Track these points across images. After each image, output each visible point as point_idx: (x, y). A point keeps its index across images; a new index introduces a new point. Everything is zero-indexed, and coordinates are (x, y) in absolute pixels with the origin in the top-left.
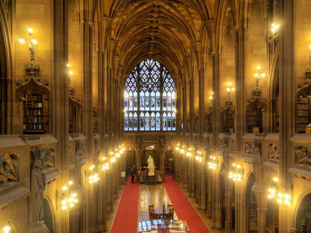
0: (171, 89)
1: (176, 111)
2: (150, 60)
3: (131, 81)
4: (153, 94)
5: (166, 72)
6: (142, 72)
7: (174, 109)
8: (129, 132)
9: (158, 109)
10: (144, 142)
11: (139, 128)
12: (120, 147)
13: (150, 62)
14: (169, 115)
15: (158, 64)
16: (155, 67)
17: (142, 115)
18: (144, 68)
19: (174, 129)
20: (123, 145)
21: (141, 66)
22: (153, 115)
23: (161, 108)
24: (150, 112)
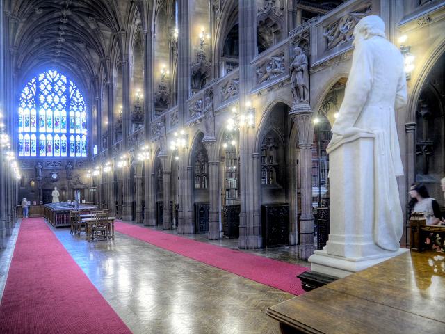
0: (81, 108)
1: (86, 134)
2: (53, 72)
3: (27, 93)
4: (57, 113)
5: (74, 87)
7: (85, 131)
9: (64, 131)
11: (38, 153)
14: (78, 138)
15: (64, 78)
22: (57, 138)
24: (53, 134)
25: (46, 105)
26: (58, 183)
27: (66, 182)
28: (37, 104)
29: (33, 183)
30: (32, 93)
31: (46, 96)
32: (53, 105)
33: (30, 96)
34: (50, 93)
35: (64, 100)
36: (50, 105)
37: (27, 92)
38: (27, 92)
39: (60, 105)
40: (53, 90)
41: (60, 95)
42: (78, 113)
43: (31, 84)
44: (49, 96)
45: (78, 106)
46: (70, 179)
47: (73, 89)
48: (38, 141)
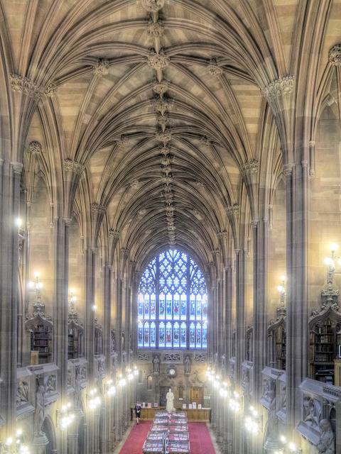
3: (147, 276)
4: (176, 297)
6: (162, 268)
7: (205, 318)
8: (144, 348)
9: (184, 318)
10: (162, 363)
11: (157, 344)
12: (129, 370)
13: (173, 253)
14: (199, 326)
15: (184, 257)
16: (180, 260)
17: (162, 325)
18: (166, 262)
19: (205, 346)
20: (136, 367)
21: (161, 259)
22: (176, 326)
23: (188, 317)
24: (173, 322)
25: (166, 289)
26: (176, 381)
27: (183, 379)
28: (158, 290)
29: (151, 378)
30: (152, 276)
31: (166, 279)
32: (173, 288)
33: (150, 279)
34: (170, 275)
35: (184, 282)
36: (170, 288)
37: (147, 275)
38: (147, 275)
39: (180, 288)
40: (173, 271)
41: (180, 276)
42: (199, 297)
43: (151, 266)
44: (169, 278)
45: (199, 289)
46: (188, 376)
47: (193, 268)
48: (157, 328)
